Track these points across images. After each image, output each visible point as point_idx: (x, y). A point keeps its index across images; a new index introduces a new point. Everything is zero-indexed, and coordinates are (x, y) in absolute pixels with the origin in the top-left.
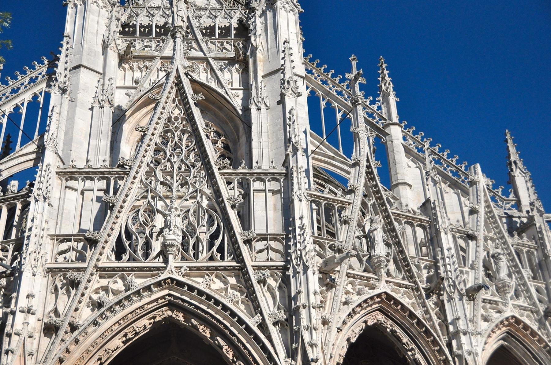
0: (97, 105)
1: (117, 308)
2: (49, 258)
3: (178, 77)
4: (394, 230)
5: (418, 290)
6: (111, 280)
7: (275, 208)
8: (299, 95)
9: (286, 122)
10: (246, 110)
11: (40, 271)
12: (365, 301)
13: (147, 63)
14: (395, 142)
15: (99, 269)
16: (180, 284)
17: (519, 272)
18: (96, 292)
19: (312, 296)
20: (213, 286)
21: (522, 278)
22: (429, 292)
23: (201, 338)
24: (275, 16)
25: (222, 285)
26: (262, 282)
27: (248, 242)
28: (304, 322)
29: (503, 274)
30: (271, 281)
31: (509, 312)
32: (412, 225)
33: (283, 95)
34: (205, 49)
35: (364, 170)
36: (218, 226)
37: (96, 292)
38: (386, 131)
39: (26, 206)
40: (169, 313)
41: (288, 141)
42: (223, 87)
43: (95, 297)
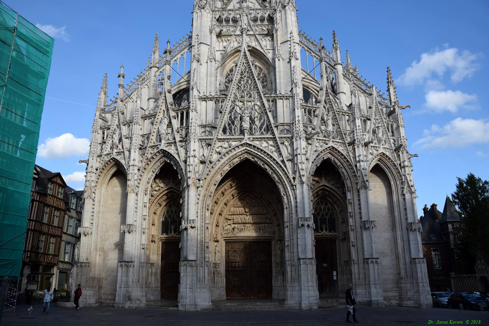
0: (209, 61)
1: (226, 155)
2: (199, 134)
3: (245, 53)
4: (336, 119)
5: (345, 144)
6: (223, 143)
7: (286, 106)
8: (297, 59)
9: (292, 71)
10: (274, 59)
11: (196, 140)
12: (324, 150)
13: (229, 38)
14: (339, 73)
15: (218, 139)
16: (250, 145)
17: (387, 133)
18: (218, 148)
19: (302, 150)
20: (263, 145)
21: (388, 136)
22: (350, 144)
23: (259, 166)
24: (285, 13)
25: (267, 145)
26: (283, 143)
27: (277, 127)
28: (299, 161)
29: (380, 135)
30: (286, 143)
31: (381, 150)
32: (344, 115)
33: (290, 60)
34: (254, 30)
35: (325, 92)
36: (264, 120)
37: (218, 148)
38: (335, 67)
39: (188, 114)
40: (246, 156)
41: (292, 82)
42: (263, 49)
43: (218, 150)
